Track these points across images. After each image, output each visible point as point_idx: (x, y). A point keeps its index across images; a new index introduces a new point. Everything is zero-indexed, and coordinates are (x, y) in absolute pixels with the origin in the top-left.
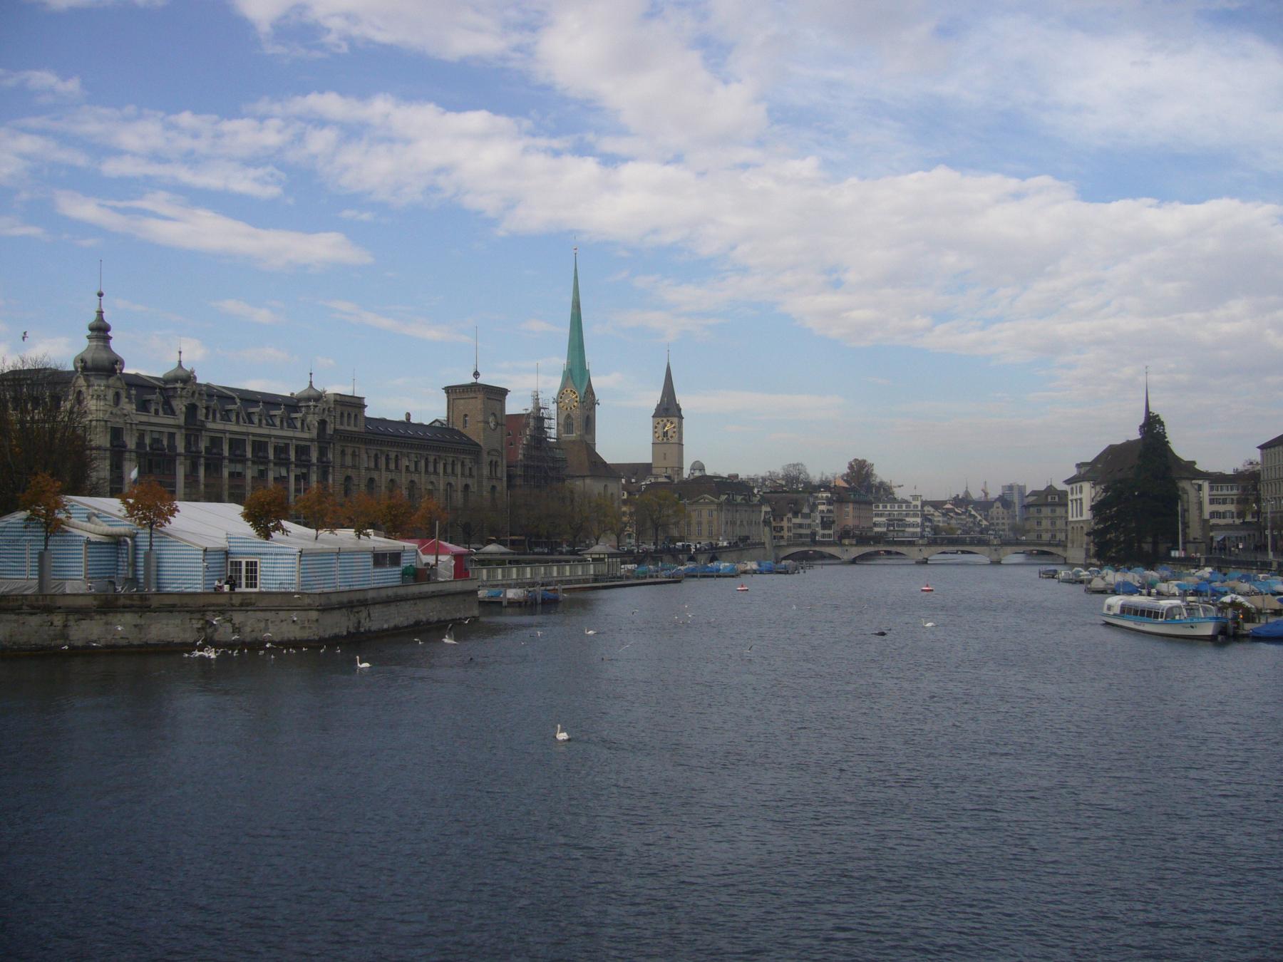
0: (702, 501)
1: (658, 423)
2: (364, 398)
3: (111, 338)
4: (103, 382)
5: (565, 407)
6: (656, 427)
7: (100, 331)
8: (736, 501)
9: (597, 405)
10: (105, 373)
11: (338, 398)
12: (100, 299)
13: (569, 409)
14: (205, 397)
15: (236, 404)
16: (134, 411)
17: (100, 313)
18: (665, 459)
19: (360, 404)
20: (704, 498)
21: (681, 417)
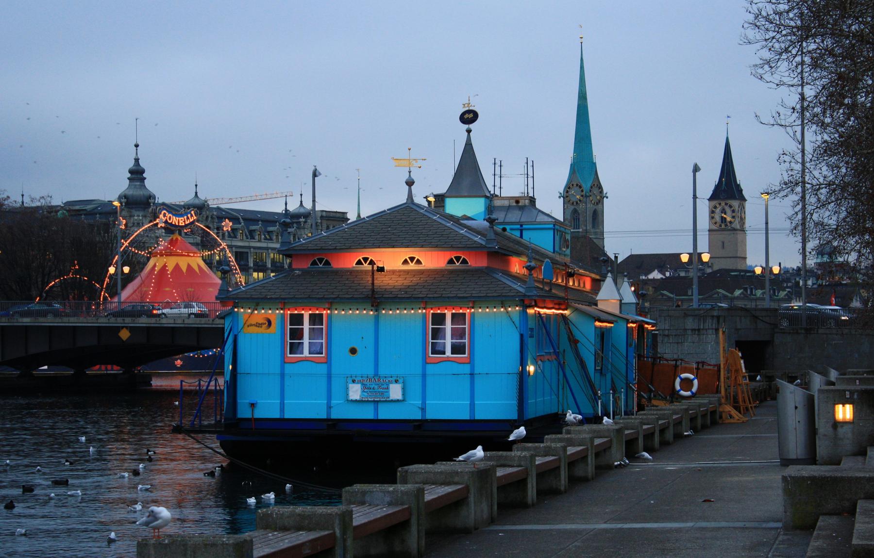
0: (716, 296)
1: (715, 207)
2: (346, 213)
3: (145, 178)
4: (141, 214)
5: (571, 202)
6: (712, 212)
7: (137, 174)
8: (755, 295)
9: (605, 198)
10: (142, 206)
11: (324, 214)
12: (137, 149)
13: (575, 203)
14: (216, 220)
15: (240, 224)
16: (164, 234)
17: (137, 160)
18: (723, 247)
19: (343, 218)
20: (718, 293)
21: (743, 199)
